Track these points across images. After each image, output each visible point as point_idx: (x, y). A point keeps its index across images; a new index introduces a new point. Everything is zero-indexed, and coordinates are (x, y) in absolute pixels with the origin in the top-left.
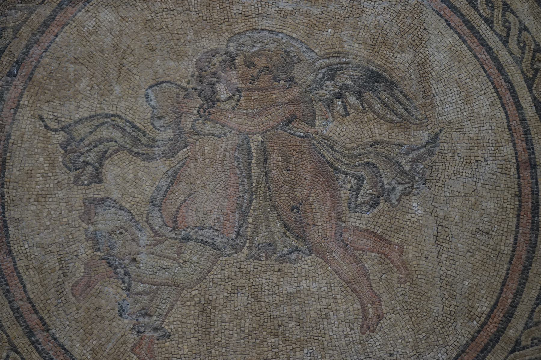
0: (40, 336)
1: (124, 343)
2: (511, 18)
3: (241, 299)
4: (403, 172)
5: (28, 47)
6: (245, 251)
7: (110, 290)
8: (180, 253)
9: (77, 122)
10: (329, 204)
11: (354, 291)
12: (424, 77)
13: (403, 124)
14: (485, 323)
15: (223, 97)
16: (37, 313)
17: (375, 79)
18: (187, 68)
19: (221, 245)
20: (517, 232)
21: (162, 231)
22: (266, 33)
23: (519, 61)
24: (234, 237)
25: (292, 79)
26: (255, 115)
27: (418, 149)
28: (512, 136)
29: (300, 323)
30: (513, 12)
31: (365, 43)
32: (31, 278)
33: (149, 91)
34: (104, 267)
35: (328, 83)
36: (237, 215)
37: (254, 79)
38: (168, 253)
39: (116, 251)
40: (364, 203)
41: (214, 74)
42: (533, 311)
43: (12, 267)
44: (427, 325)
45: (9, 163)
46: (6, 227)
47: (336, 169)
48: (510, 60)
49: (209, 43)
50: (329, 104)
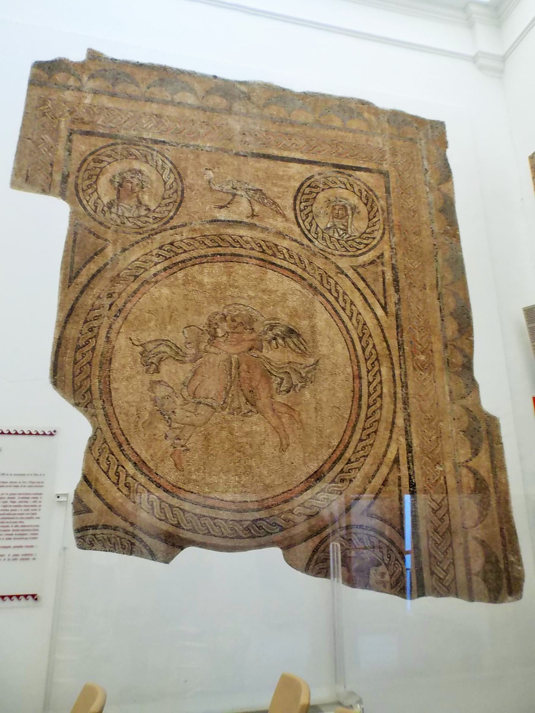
0: (125, 447)
1: (167, 452)
2: (353, 308)
3: (224, 434)
5: (125, 303)
6: (227, 410)
8: (196, 410)
9: (148, 342)
10: (267, 390)
11: (277, 432)
12: (313, 332)
13: (303, 354)
14: (335, 450)
15: (220, 335)
16: (124, 435)
18: (203, 320)
19: (215, 407)
20: (352, 408)
22: (242, 306)
23: (356, 329)
24: (222, 403)
25: (253, 329)
26: (235, 345)
27: (309, 366)
28: (351, 363)
29: (251, 446)
30: (354, 305)
32: (122, 418)
33: (185, 330)
34: (159, 415)
35: (269, 332)
36: (224, 393)
37: (236, 327)
38: (190, 409)
39: (165, 407)
40: (284, 391)
41: (216, 324)
42: (357, 445)
43: (113, 413)
44: (310, 449)
46: (110, 392)
47: (271, 373)
49: (214, 308)
50: (270, 342)
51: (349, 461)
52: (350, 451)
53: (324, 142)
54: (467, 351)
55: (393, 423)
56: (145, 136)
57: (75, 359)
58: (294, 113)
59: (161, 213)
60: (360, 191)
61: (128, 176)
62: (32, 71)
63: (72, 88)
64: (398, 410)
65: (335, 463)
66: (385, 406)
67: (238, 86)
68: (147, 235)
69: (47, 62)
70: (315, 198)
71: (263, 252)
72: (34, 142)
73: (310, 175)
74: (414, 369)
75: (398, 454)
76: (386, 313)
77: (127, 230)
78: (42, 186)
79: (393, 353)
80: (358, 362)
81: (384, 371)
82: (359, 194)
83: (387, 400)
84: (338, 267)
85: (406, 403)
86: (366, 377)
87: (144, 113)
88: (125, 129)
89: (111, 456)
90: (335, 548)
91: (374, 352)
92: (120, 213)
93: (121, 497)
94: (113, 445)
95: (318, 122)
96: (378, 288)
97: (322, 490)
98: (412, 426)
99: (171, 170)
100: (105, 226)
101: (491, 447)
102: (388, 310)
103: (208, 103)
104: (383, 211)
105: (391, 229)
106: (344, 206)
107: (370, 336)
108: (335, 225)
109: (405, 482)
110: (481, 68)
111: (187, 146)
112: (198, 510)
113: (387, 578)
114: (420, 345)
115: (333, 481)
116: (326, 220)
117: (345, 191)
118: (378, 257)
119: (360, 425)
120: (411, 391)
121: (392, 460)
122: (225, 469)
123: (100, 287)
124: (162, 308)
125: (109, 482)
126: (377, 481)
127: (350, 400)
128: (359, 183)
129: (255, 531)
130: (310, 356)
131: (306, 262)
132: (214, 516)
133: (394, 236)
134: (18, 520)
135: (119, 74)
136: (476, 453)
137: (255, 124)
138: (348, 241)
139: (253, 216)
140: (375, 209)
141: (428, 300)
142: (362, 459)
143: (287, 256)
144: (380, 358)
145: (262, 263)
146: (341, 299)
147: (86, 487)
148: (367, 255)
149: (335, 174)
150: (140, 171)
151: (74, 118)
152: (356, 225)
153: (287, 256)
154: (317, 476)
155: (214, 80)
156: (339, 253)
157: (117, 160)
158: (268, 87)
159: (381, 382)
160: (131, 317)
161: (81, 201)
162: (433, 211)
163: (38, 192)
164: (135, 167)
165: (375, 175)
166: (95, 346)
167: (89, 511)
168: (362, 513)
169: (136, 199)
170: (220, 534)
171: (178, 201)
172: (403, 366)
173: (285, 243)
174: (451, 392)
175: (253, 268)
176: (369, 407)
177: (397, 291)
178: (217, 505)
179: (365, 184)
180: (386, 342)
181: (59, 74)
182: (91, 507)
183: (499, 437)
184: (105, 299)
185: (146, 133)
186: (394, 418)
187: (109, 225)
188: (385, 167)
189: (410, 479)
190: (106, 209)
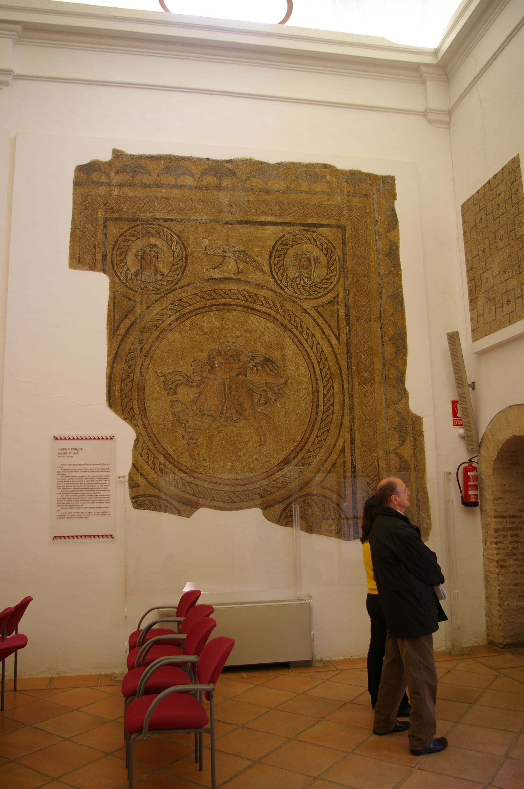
0: (157, 445)
2: (314, 339)
4: (275, 393)
6: (223, 418)
7: (179, 431)
8: (202, 419)
11: (258, 432)
12: (284, 360)
13: (276, 376)
15: (217, 366)
17: (267, 360)
21: (196, 412)
23: (316, 355)
25: (240, 360)
29: (240, 443)
31: (264, 347)
32: (154, 426)
34: (177, 423)
37: (227, 359)
39: (181, 418)
41: (214, 357)
45: (146, 388)
48: (313, 355)
49: (212, 347)
50: (252, 369)
51: (309, 451)
52: (309, 444)
53: (293, 205)
54: (401, 368)
55: (342, 423)
56: (157, 217)
57: (121, 388)
58: (270, 182)
59: (171, 276)
60: (322, 244)
61: (147, 250)
62: (75, 174)
63: (104, 184)
64: (345, 414)
65: (298, 453)
66: (336, 412)
67: (226, 164)
68: (163, 295)
69: (85, 165)
70: (286, 253)
71: (247, 300)
72: (81, 231)
73: (282, 234)
74: (359, 383)
75: (344, 445)
76: (339, 342)
77: (149, 292)
78: (90, 265)
79: (343, 372)
80: (317, 380)
81: (336, 386)
82: (320, 247)
83: (337, 407)
84: (303, 308)
85: (351, 409)
86: (322, 391)
87: (156, 198)
88: (143, 213)
89: (149, 451)
90: (296, 509)
91: (329, 372)
92: (143, 280)
93: (157, 477)
94: (150, 444)
95: (288, 188)
96: (334, 324)
97: (289, 471)
98: (355, 425)
99: (177, 242)
100: (134, 291)
101: (415, 439)
102: (341, 339)
103: (203, 183)
104: (339, 259)
105: (345, 274)
106: (309, 259)
107: (326, 360)
108: (301, 275)
109: (349, 464)
110: (430, 121)
111: (188, 221)
112: (206, 485)
113: (333, 527)
114: (364, 364)
115: (297, 465)
116: (294, 271)
117: (309, 245)
118: (334, 298)
119: (317, 426)
120: (356, 400)
121: (339, 450)
122: (223, 458)
123: (134, 335)
124: (176, 349)
125: (149, 468)
126: (328, 465)
127: (310, 408)
128: (320, 237)
129: (244, 498)
130: (282, 377)
131: (279, 306)
132: (217, 488)
133: (348, 279)
134: (97, 492)
135: (136, 167)
136: (402, 443)
137: (239, 196)
138: (311, 286)
139: (238, 272)
140: (333, 259)
141: (372, 330)
142: (318, 450)
143: (264, 302)
144: (333, 377)
145: (245, 310)
146: (304, 333)
147: (135, 472)
148: (325, 297)
149: (301, 232)
150: (155, 245)
151: (107, 209)
152: (318, 273)
153: (264, 302)
154: (286, 462)
155: (207, 162)
156: (304, 297)
157: (139, 238)
158: (249, 163)
159: (333, 394)
160: (154, 357)
161: (116, 273)
162: (381, 256)
163: (87, 270)
164: (152, 242)
165: (334, 230)
166: (133, 378)
167: (139, 486)
168: (317, 486)
169: (153, 267)
170: (221, 500)
171: (184, 266)
172: (350, 382)
173: (263, 293)
174: (386, 400)
175: (239, 314)
176: (324, 413)
177: (348, 324)
178: (218, 482)
179: (326, 238)
180: (339, 364)
181: (94, 174)
182: (140, 484)
183: (422, 431)
184: (137, 344)
185: (158, 214)
186: (342, 419)
187: (137, 290)
188: (343, 221)
189: (352, 462)
190: (133, 277)
